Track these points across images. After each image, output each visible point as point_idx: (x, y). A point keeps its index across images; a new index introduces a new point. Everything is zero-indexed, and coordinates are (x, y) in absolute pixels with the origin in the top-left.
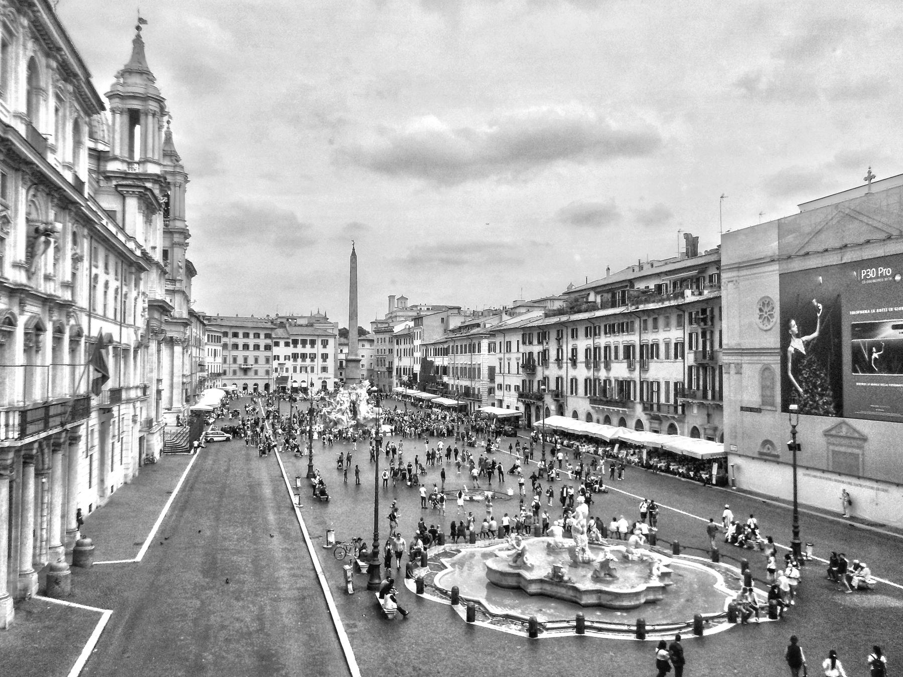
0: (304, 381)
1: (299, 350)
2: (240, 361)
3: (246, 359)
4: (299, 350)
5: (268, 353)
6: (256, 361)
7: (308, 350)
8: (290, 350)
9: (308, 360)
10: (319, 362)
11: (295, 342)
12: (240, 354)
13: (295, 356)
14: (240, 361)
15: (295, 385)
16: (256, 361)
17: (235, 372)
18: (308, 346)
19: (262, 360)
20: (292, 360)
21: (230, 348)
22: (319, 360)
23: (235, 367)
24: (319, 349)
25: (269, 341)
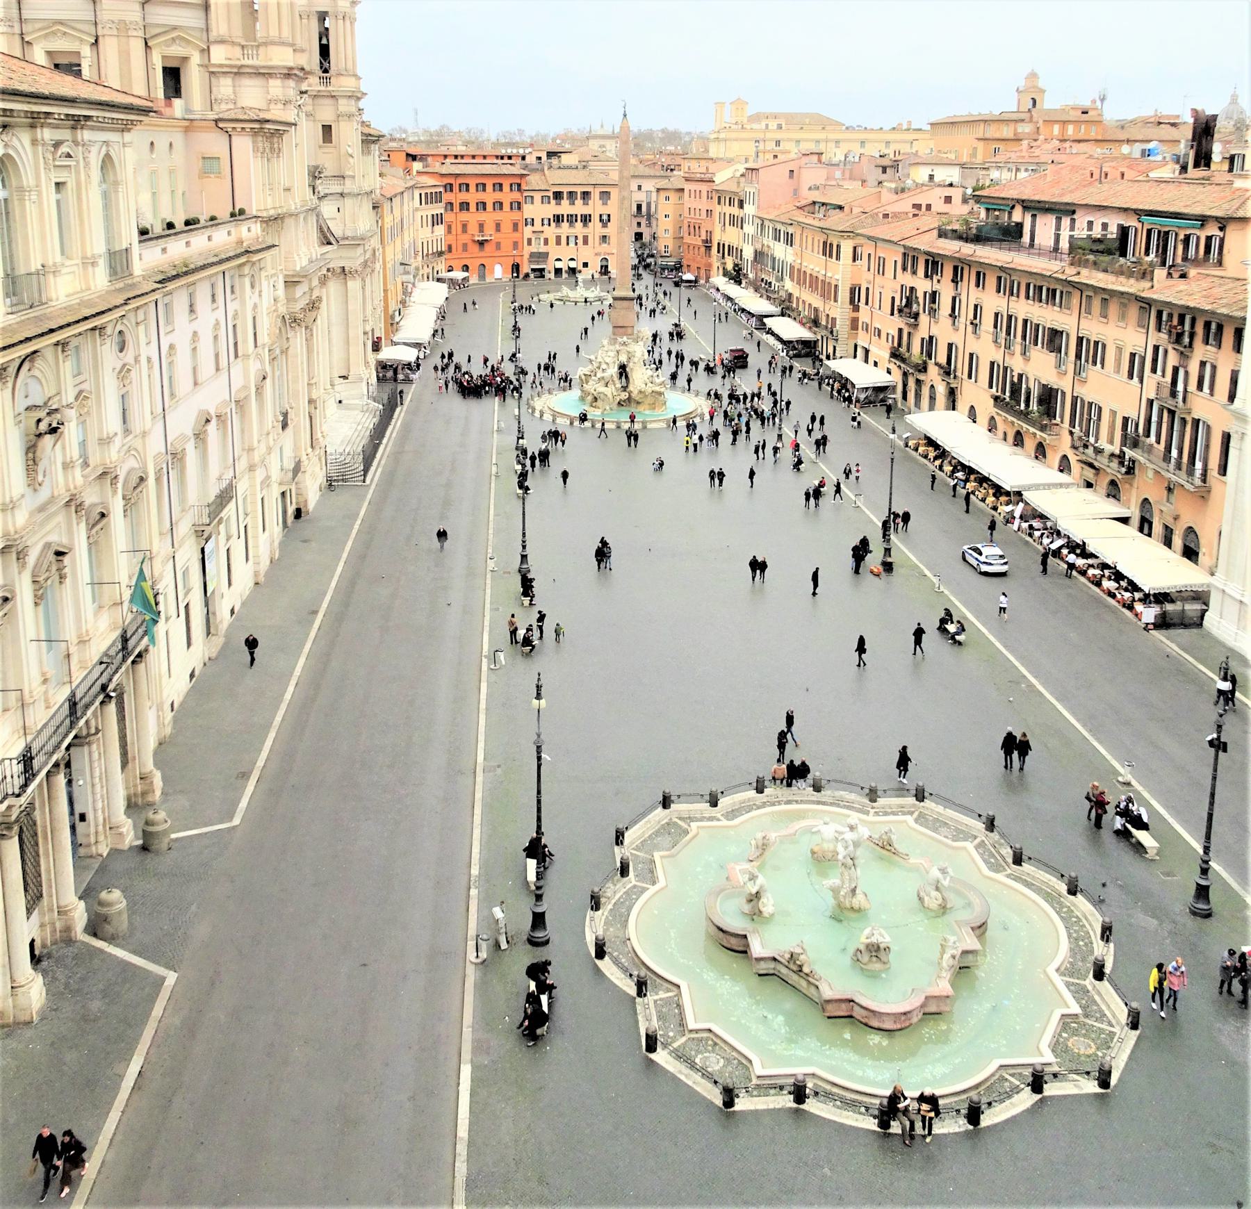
0: (572, 259)
1: (565, 208)
2: (473, 229)
3: (481, 227)
4: (565, 208)
5: (515, 215)
6: (498, 227)
7: (579, 208)
8: (552, 209)
9: (579, 224)
10: (595, 228)
11: (558, 196)
12: (472, 217)
13: (558, 219)
14: (473, 229)
15: (559, 265)
16: (498, 227)
17: (465, 246)
18: (579, 202)
19: (507, 227)
20: (553, 224)
21: (456, 207)
22: (595, 224)
23: (465, 238)
24: (595, 207)
25: (516, 196)
